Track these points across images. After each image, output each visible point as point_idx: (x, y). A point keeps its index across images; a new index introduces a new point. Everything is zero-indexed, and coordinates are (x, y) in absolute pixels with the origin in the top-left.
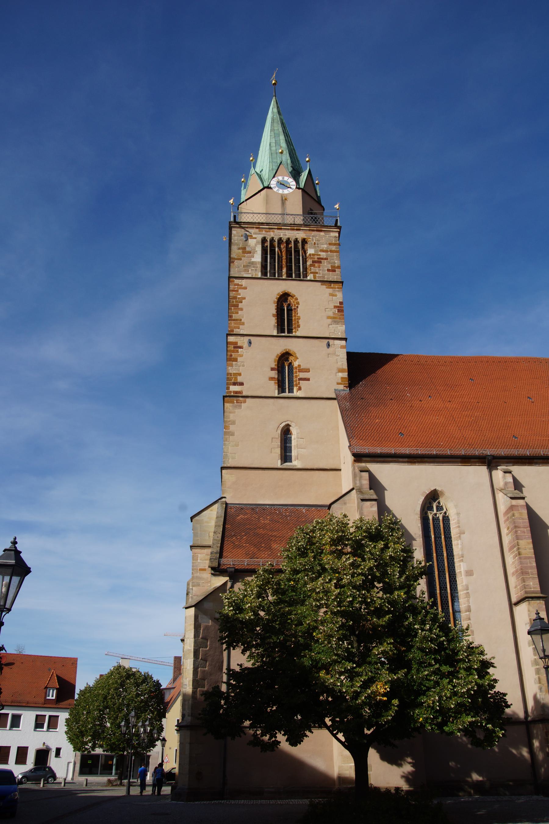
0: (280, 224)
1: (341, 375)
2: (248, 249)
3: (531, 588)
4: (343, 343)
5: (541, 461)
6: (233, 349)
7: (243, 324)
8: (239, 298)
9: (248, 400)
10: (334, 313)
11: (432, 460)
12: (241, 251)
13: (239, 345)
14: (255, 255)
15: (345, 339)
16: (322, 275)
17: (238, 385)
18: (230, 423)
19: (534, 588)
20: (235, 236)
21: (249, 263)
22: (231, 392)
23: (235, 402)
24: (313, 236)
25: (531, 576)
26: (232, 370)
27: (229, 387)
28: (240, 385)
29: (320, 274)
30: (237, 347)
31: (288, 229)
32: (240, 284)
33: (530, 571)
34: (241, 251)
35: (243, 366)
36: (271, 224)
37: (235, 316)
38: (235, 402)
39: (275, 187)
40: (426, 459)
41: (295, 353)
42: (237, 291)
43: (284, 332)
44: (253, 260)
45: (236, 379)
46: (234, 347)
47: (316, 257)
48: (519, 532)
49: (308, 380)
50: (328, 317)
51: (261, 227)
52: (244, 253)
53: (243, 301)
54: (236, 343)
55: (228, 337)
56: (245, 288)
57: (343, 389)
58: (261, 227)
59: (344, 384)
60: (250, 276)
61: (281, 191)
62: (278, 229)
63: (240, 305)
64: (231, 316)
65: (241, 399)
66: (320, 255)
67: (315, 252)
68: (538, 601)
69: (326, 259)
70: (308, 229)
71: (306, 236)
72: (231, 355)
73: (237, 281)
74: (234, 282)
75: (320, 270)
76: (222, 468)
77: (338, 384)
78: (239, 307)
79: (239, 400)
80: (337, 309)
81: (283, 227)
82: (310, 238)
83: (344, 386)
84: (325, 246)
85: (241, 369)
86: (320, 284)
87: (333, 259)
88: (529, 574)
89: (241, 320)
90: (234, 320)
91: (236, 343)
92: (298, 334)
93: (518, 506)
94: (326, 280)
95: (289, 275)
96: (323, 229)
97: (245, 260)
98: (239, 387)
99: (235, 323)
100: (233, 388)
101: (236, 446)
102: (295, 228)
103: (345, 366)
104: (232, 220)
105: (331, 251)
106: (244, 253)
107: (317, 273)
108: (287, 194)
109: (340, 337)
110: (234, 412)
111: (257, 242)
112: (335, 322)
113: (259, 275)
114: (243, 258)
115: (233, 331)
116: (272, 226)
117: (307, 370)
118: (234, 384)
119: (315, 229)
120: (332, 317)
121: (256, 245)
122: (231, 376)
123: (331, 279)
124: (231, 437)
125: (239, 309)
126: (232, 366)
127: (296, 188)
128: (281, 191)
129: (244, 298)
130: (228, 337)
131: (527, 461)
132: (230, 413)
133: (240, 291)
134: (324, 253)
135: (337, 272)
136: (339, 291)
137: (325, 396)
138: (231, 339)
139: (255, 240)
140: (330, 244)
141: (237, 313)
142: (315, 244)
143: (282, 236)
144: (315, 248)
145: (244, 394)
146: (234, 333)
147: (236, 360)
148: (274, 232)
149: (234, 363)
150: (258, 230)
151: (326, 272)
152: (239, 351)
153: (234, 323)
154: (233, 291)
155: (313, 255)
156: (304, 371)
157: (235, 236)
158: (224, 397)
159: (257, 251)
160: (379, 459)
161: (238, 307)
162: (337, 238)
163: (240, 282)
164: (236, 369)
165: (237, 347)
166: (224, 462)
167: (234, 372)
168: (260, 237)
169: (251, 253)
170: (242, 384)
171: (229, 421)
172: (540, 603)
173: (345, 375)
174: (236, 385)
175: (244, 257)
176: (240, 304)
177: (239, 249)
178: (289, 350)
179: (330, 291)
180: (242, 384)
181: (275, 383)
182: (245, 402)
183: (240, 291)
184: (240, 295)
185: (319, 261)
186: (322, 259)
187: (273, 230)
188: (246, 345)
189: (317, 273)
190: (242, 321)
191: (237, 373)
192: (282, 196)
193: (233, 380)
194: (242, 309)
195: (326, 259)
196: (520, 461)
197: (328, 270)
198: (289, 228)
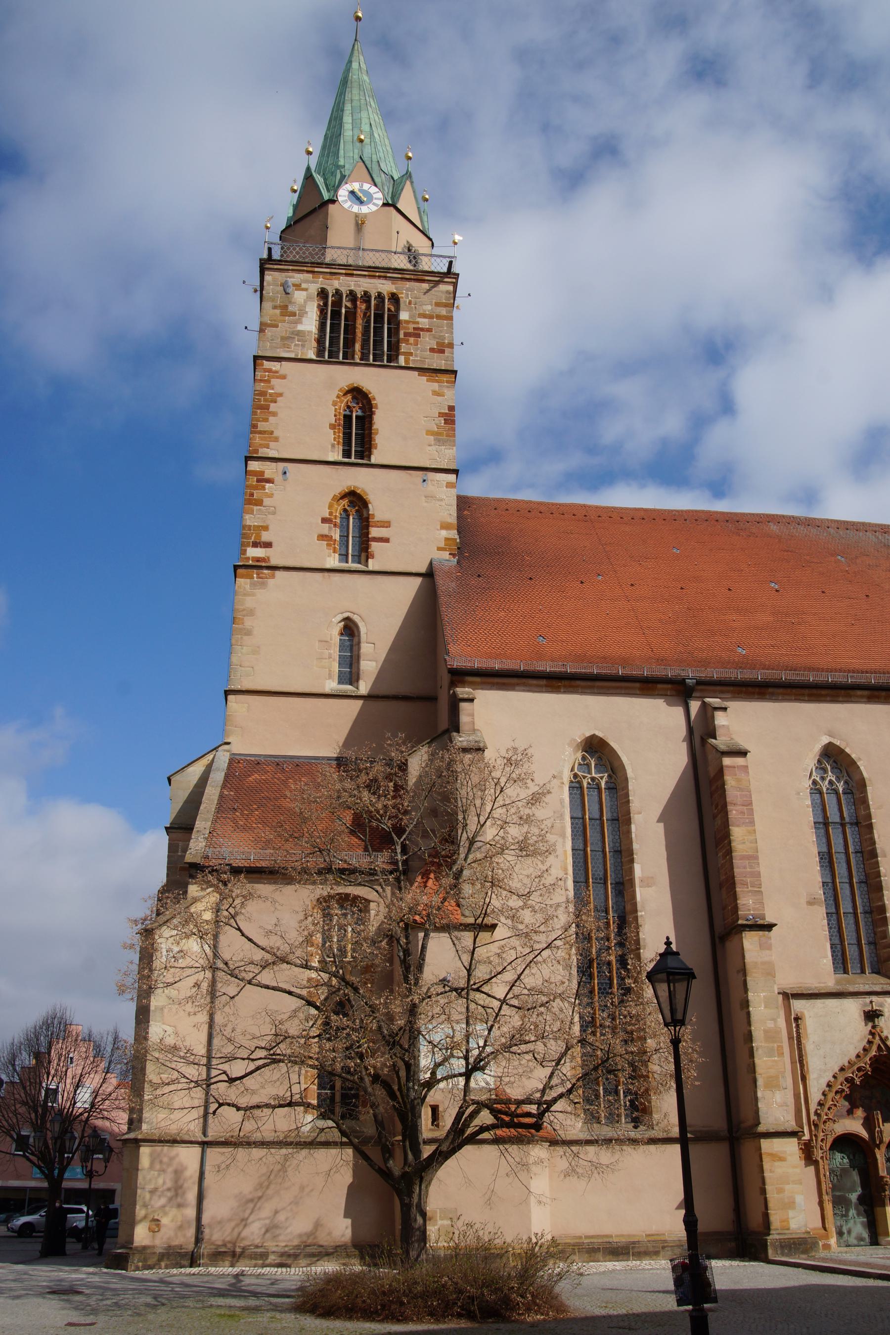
0: (350, 266)
1: (444, 533)
2: (291, 308)
3: (749, 910)
4: (452, 477)
5: (781, 690)
6: (255, 483)
7: (276, 439)
8: (271, 395)
9: (279, 574)
10: (438, 426)
11: (589, 683)
12: (278, 312)
13: (267, 476)
14: (304, 319)
15: (456, 472)
16: (421, 357)
17: (261, 547)
18: (245, 612)
19: (754, 909)
20: (269, 285)
21: (293, 333)
22: (248, 559)
23: (255, 576)
24: (407, 290)
25: (750, 888)
26: (250, 520)
27: (246, 550)
28: (264, 547)
29: (416, 356)
30: (263, 480)
31: (365, 276)
32: (274, 369)
33: (749, 880)
34: (278, 312)
35: (274, 513)
36: (334, 265)
37: (262, 426)
38: (255, 576)
39: (346, 201)
40: (578, 683)
41: (365, 492)
42: (268, 381)
43: (350, 457)
44: (300, 327)
45: (259, 536)
46: (258, 481)
47: (411, 326)
48: (734, 812)
49: (387, 540)
50: (429, 433)
51: (316, 269)
52: (282, 315)
53: (279, 399)
54: (262, 473)
55: (249, 462)
56: (284, 377)
57: (447, 558)
58: (316, 269)
59: (450, 549)
60: (292, 355)
61: (356, 209)
62: (347, 275)
63: (273, 407)
64: (255, 426)
65: (266, 571)
66: (418, 323)
67: (410, 317)
68: (761, 933)
69: (429, 330)
70: (400, 276)
71: (396, 289)
72: (252, 495)
73: (267, 364)
74: (263, 365)
75: (417, 349)
76: (227, 693)
77: (439, 549)
78: (270, 410)
79: (262, 573)
80: (443, 419)
81: (355, 272)
82: (402, 293)
83: (450, 554)
84: (429, 307)
85: (271, 521)
86: (416, 373)
87: (441, 331)
88: (747, 885)
89: (272, 433)
90: (260, 432)
91: (262, 473)
92: (373, 460)
93: (734, 767)
94: (426, 367)
95: (364, 357)
96: (427, 278)
97: (283, 328)
98: (264, 550)
99: (261, 439)
100: (253, 552)
101: (254, 654)
102: (377, 274)
103: (453, 520)
104: (265, 256)
105: (439, 317)
106: (282, 315)
107: (411, 354)
108: (366, 215)
109: (446, 467)
110: (253, 595)
111: (309, 298)
112: (439, 441)
113: (312, 355)
114: (280, 324)
115: (257, 451)
116: (335, 268)
117: (386, 524)
118: (255, 545)
119: (412, 277)
120: (434, 432)
121: (305, 302)
122: (250, 530)
123: (434, 366)
124: (245, 638)
125: (270, 413)
126: (252, 512)
127: (385, 205)
128: (356, 209)
129: (281, 395)
130: (249, 462)
131: (757, 690)
132: (245, 595)
133: (274, 382)
134: (426, 320)
135: (446, 354)
136: (448, 387)
137: (414, 571)
138: (254, 466)
139: (304, 293)
140: (438, 304)
141: (266, 420)
142: (410, 303)
143: (352, 288)
144: (410, 310)
145: (274, 562)
146: (260, 455)
147: (259, 503)
148: (339, 279)
149: (255, 508)
150: (310, 276)
151: (428, 353)
152: (267, 487)
153: (259, 437)
154: (261, 381)
155: (407, 322)
156: (379, 525)
157: (269, 285)
158: (236, 567)
159: (306, 313)
160: (496, 680)
161: (268, 409)
162: (450, 293)
163: (275, 366)
164: (258, 518)
165: (263, 480)
166: (228, 679)
167: (256, 524)
168: (314, 288)
169: (295, 316)
170: (268, 545)
171: (244, 610)
172: (764, 935)
173: (453, 534)
174: (257, 547)
175: (284, 321)
176: (272, 405)
177: (275, 307)
178: (354, 487)
179: (435, 386)
180: (268, 545)
181: (328, 545)
182: (273, 577)
183: (274, 382)
184: (273, 389)
185: (417, 333)
186: (422, 330)
187: (337, 276)
188: (278, 478)
189: (411, 354)
190: (276, 434)
191: (261, 526)
192: (357, 216)
193: (253, 538)
194: (274, 414)
195: (429, 330)
196: (744, 689)
197: (432, 350)
198: (366, 273)
